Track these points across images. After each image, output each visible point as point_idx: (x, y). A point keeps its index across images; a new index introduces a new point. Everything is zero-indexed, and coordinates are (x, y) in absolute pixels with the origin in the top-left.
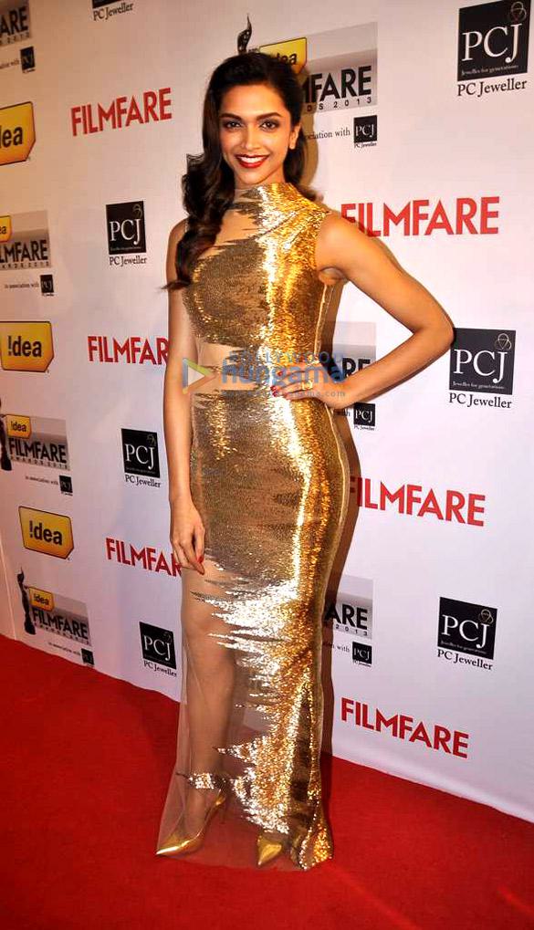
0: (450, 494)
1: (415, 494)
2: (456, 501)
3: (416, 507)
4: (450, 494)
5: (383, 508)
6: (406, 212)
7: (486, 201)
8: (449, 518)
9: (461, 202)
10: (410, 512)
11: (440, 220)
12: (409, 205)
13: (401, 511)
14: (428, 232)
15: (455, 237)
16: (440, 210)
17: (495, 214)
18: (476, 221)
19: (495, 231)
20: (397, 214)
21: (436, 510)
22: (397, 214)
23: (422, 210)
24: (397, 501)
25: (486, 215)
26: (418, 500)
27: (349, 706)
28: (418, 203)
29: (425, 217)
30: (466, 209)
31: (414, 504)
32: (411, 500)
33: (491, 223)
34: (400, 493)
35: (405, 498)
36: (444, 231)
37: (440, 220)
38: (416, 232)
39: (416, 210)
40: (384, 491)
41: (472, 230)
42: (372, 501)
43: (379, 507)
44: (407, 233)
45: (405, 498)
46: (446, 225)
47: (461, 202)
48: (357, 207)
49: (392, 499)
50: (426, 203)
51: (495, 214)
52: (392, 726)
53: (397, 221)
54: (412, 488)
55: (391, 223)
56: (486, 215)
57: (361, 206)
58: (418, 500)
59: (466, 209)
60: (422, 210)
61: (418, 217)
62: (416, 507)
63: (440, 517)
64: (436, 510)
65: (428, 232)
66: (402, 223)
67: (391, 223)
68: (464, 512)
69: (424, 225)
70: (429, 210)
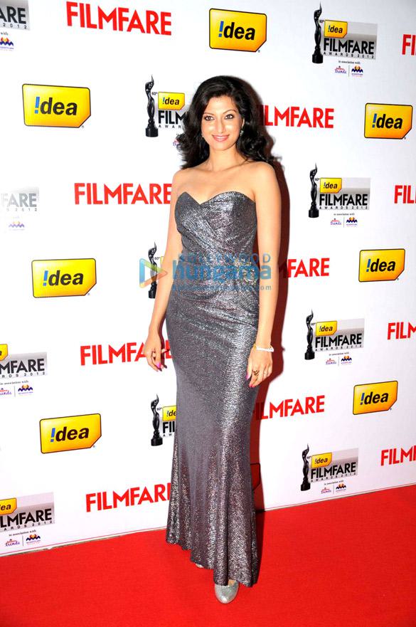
0: (152, 186)
1: (129, 189)
2: (155, 190)
3: (130, 198)
4: (152, 186)
5: (107, 202)
6: (113, 14)
7: (164, 14)
8: (152, 202)
9: (149, 13)
10: (126, 202)
11: (136, 23)
12: (115, 10)
13: (120, 202)
14: (129, 30)
15: (146, 34)
16: (136, 16)
17: (169, 23)
18: (158, 25)
19: (169, 33)
20: (108, 15)
21: (144, 198)
22: (108, 15)
23: (124, 14)
24: (117, 196)
25: (164, 23)
26: (131, 193)
27: (86, 351)
28: (122, 10)
30: (152, 18)
32: (126, 194)
33: (167, 28)
34: (119, 189)
36: (139, 30)
37: (136, 23)
38: (121, 29)
40: (107, 190)
41: (157, 32)
42: (99, 199)
44: (115, 28)
46: (140, 26)
47: (149, 13)
48: (79, 5)
49: (113, 195)
50: (127, 10)
51: (169, 23)
53: (108, 20)
54: (126, 186)
55: (104, 20)
56: (164, 23)
58: (131, 193)
59: (152, 18)
60: (124, 14)
61: (122, 19)
62: (130, 198)
63: (146, 203)
64: (144, 198)
65: (129, 30)
66: (112, 21)
67: (104, 20)
68: (161, 196)
69: (126, 25)
70: (129, 15)
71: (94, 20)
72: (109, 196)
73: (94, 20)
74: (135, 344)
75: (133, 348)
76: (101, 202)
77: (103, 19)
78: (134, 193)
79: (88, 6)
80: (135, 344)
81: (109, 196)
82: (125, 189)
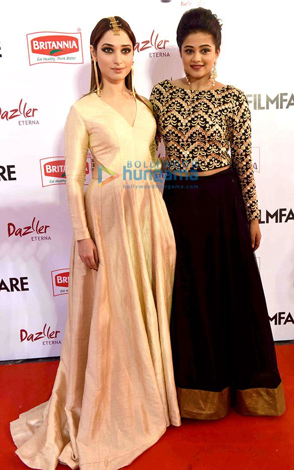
5: (268, 222)
10: (281, 221)
13: (277, 222)
23: (284, 97)
26: (285, 215)
29: (286, 100)
31: (283, 217)
32: (281, 215)
34: (276, 214)
35: (278, 216)
39: (281, 98)
40: (268, 214)
43: (266, 222)
45: (278, 216)
49: (272, 217)
52: (274, 320)
54: (281, 210)
57: (255, 96)
71: (263, 104)
72: (269, 217)
73: (263, 104)
74: (284, 313)
75: (282, 316)
76: (264, 222)
77: (269, 102)
78: (287, 215)
79: (259, 96)
80: (284, 313)
81: (269, 217)
82: (281, 213)
